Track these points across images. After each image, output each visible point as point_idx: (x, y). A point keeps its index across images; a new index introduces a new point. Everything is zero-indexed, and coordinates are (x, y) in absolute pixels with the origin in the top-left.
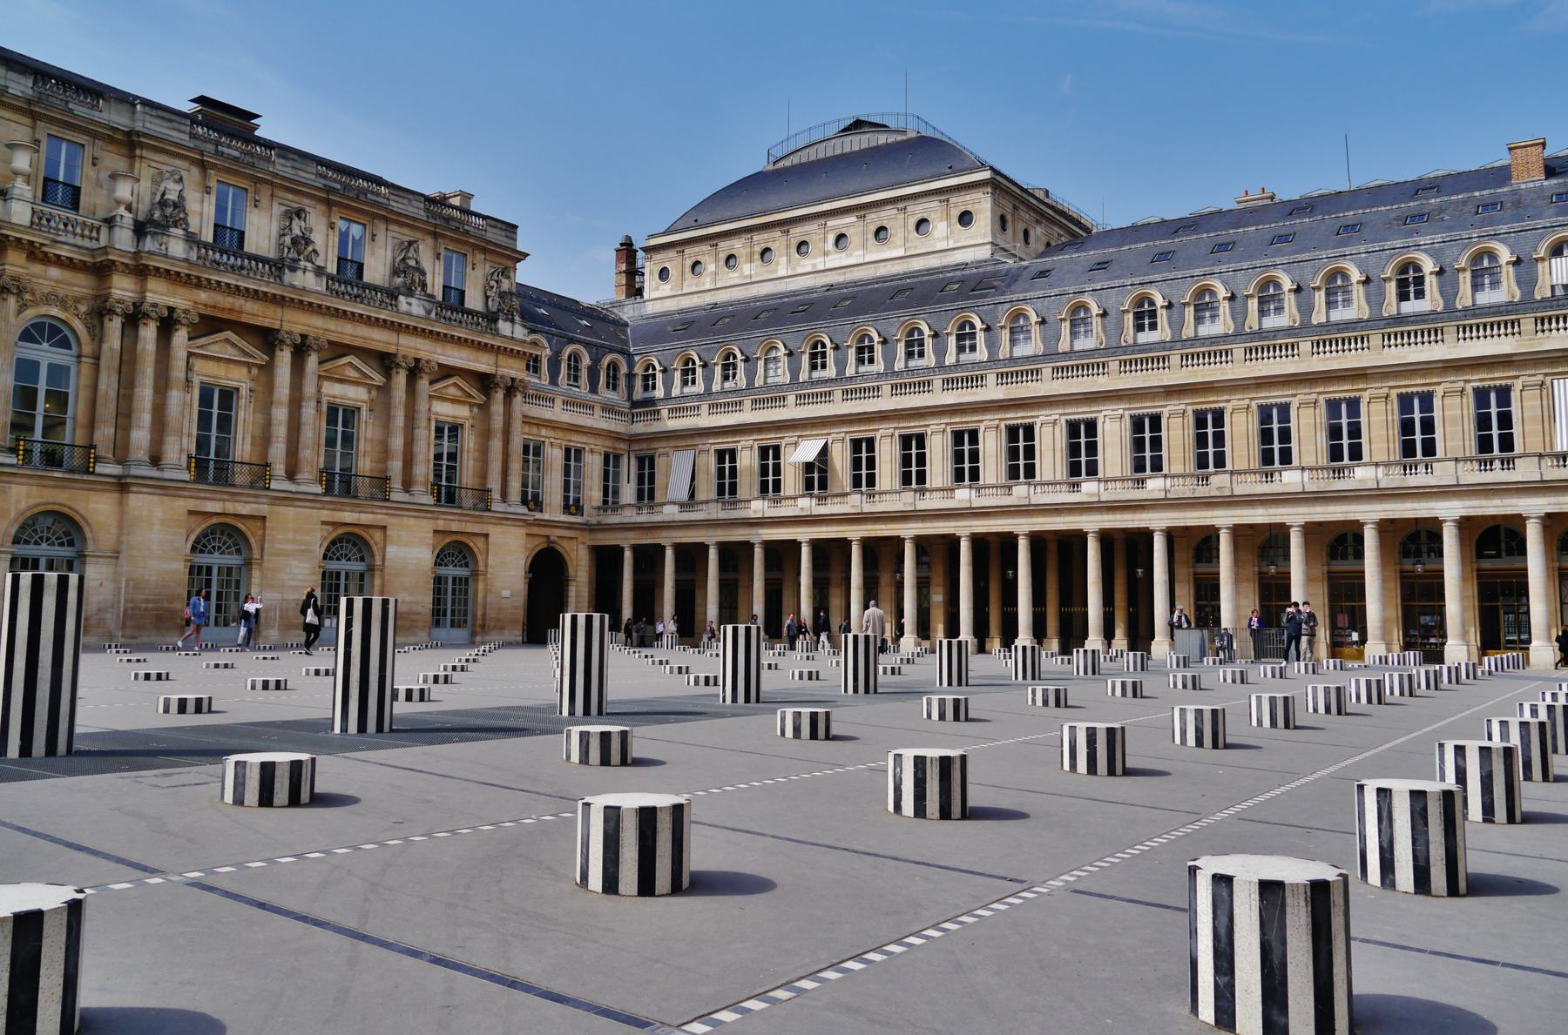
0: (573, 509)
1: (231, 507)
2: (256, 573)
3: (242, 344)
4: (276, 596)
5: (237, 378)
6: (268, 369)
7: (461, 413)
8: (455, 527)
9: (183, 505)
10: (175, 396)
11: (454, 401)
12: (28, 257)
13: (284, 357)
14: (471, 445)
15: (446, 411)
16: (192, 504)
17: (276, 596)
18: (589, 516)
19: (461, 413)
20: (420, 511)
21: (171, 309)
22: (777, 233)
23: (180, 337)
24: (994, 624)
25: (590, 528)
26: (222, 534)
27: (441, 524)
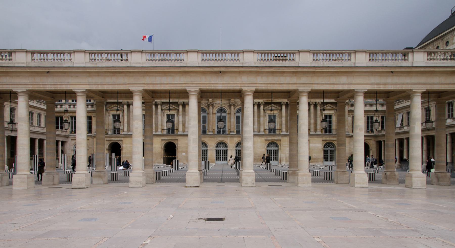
0: (370, 132)
1: (273, 138)
2: (280, 151)
3: (275, 106)
4: (284, 155)
5: (276, 113)
6: (281, 110)
7: (331, 112)
8: (328, 139)
9: (264, 139)
10: (262, 119)
11: (329, 110)
13: (284, 107)
14: (335, 119)
15: (327, 112)
16: (266, 138)
17: (284, 155)
18: (375, 133)
19: (331, 112)
20: (318, 136)
21: (259, 103)
22: (440, 41)
23: (262, 107)
24: (223, 155)
25: (375, 137)
26: (272, 144)
27: (324, 138)
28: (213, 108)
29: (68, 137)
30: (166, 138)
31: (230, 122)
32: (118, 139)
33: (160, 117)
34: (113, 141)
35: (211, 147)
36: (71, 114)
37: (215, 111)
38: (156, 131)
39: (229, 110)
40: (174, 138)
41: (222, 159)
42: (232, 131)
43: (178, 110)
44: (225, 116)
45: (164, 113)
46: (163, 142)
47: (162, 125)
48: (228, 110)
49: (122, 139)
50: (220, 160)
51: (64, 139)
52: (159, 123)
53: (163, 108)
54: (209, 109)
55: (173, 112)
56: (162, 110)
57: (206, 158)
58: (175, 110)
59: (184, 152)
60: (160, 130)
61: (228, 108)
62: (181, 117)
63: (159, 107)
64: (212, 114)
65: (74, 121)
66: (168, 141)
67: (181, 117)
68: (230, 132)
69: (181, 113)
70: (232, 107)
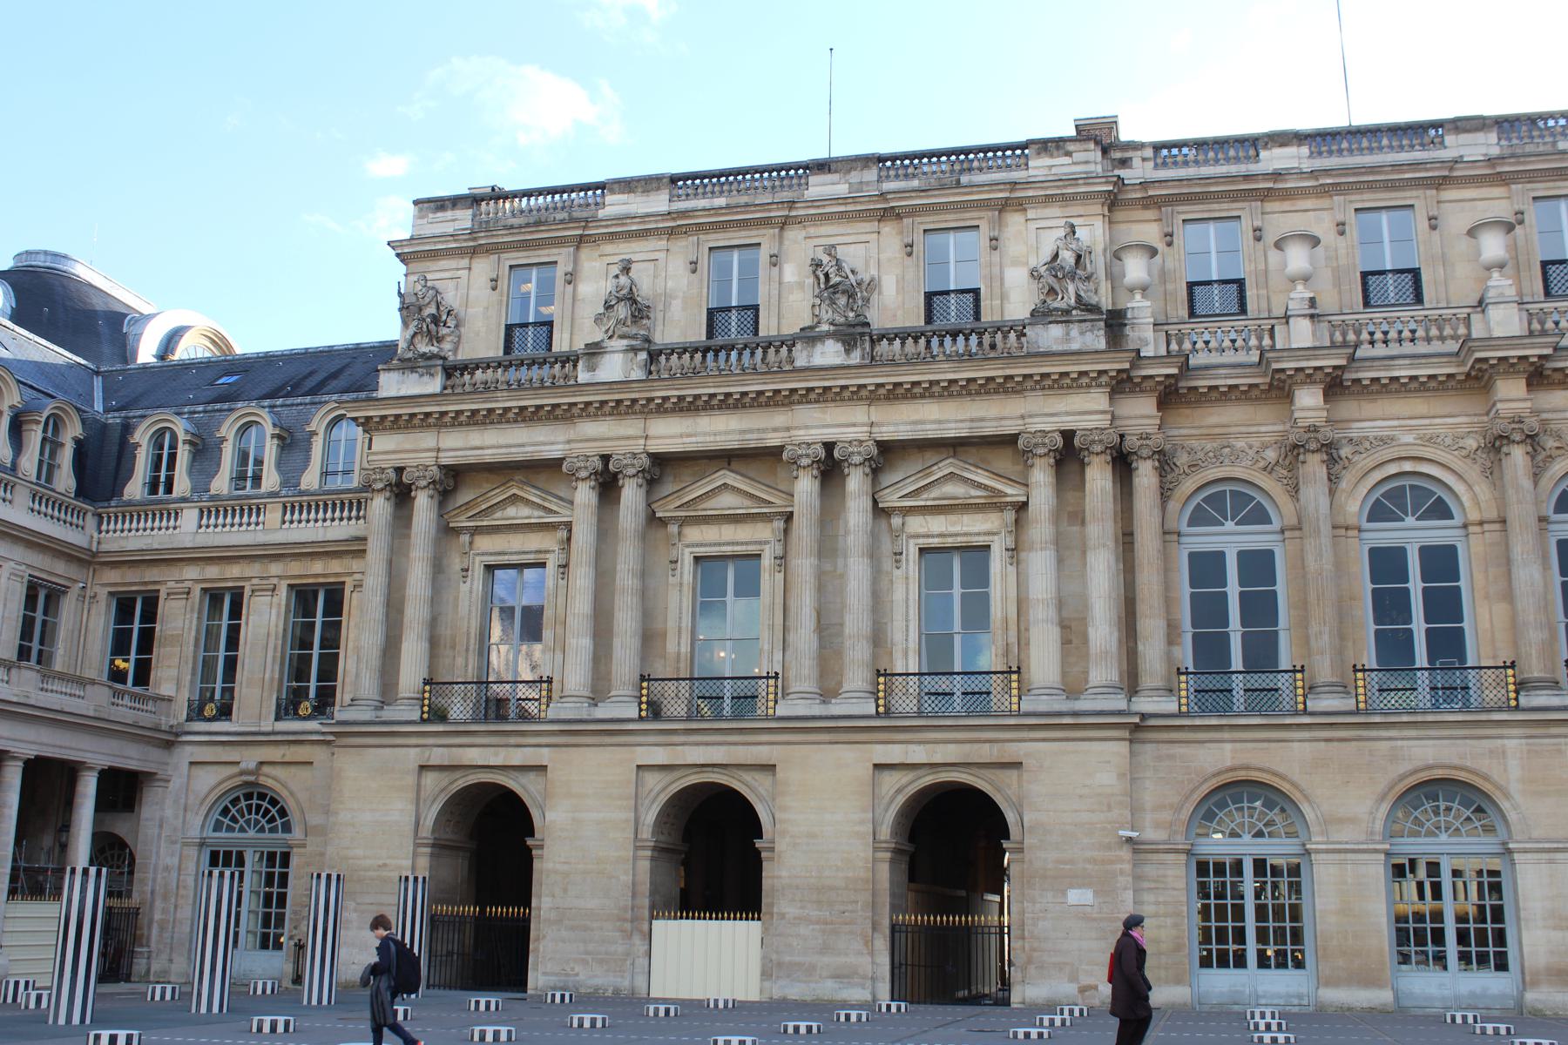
12: (1530, 385)
28: (1333, 479)
29: (169, 741)
30: (918, 754)
31: (1509, 596)
32: (517, 757)
33: (857, 572)
34: (473, 778)
35: (1345, 835)
36: (212, 571)
37: (1354, 505)
38: (827, 693)
39: (1483, 490)
40: (985, 753)
41: (1452, 947)
42: (1535, 671)
43: (1022, 507)
44: (1451, 551)
45: (896, 535)
46: (891, 781)
47: (878, 638)
48: (1471, 494)
49: (543, 756)
50: (1440, 959)
51: (131, 757)
52: (856, 622)
53: (891, 499)
54: (1294, 491)
55: (972, 527)
56: (880, 511)
57: (1297, 936)
58: (994, 504)
59: (1080, 880)
60: (856, 678)
61: (1473, 472)
62: (1040, 563)
63: (856, 482)
64: (1325, 529)
65: (225, 622)
66: (928, 779)
67: (1040, 563)
68: (1521, 686)
69: (1041, 525)
70: (1518, 455)
